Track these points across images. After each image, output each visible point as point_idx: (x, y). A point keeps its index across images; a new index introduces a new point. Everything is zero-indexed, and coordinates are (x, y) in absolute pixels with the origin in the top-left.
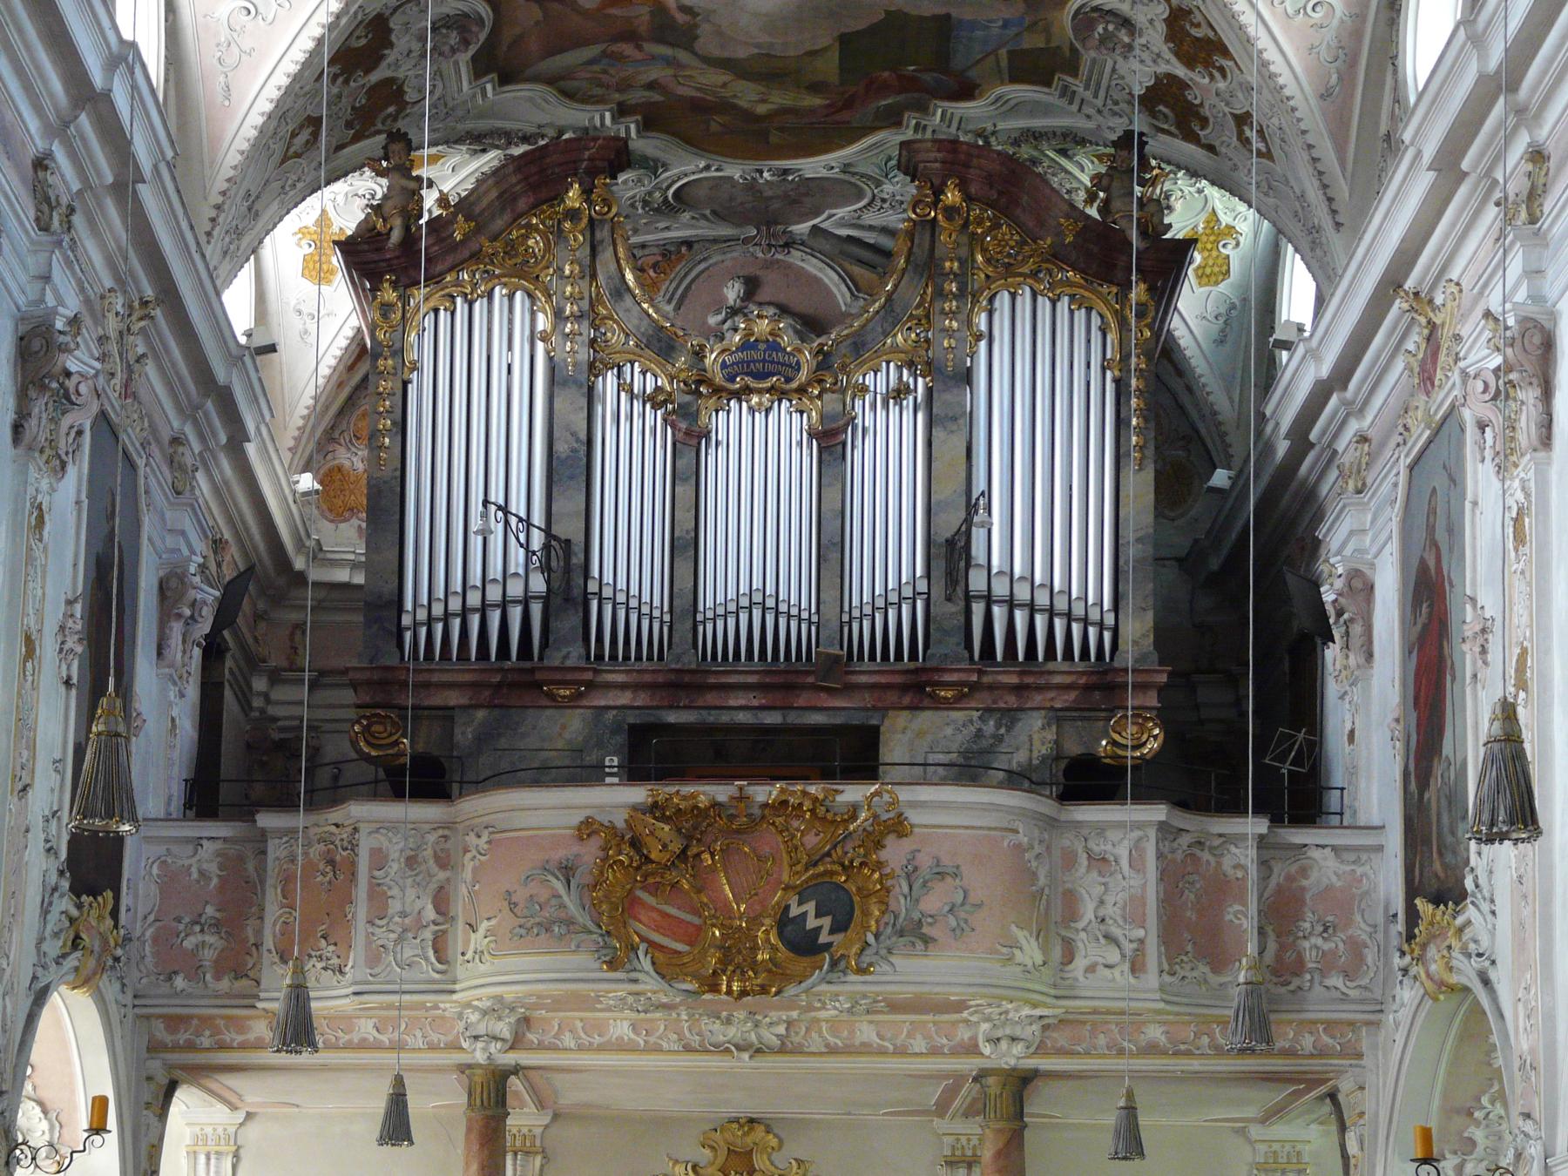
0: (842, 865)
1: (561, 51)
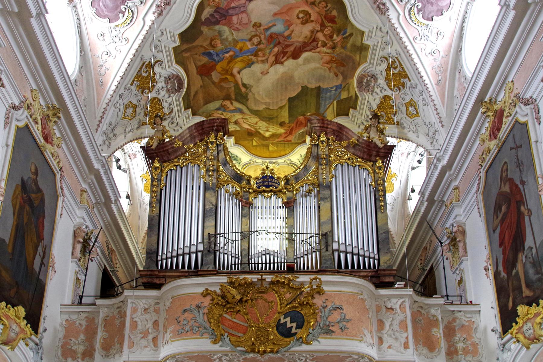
0: (300, 304)
1: (209, 102)
